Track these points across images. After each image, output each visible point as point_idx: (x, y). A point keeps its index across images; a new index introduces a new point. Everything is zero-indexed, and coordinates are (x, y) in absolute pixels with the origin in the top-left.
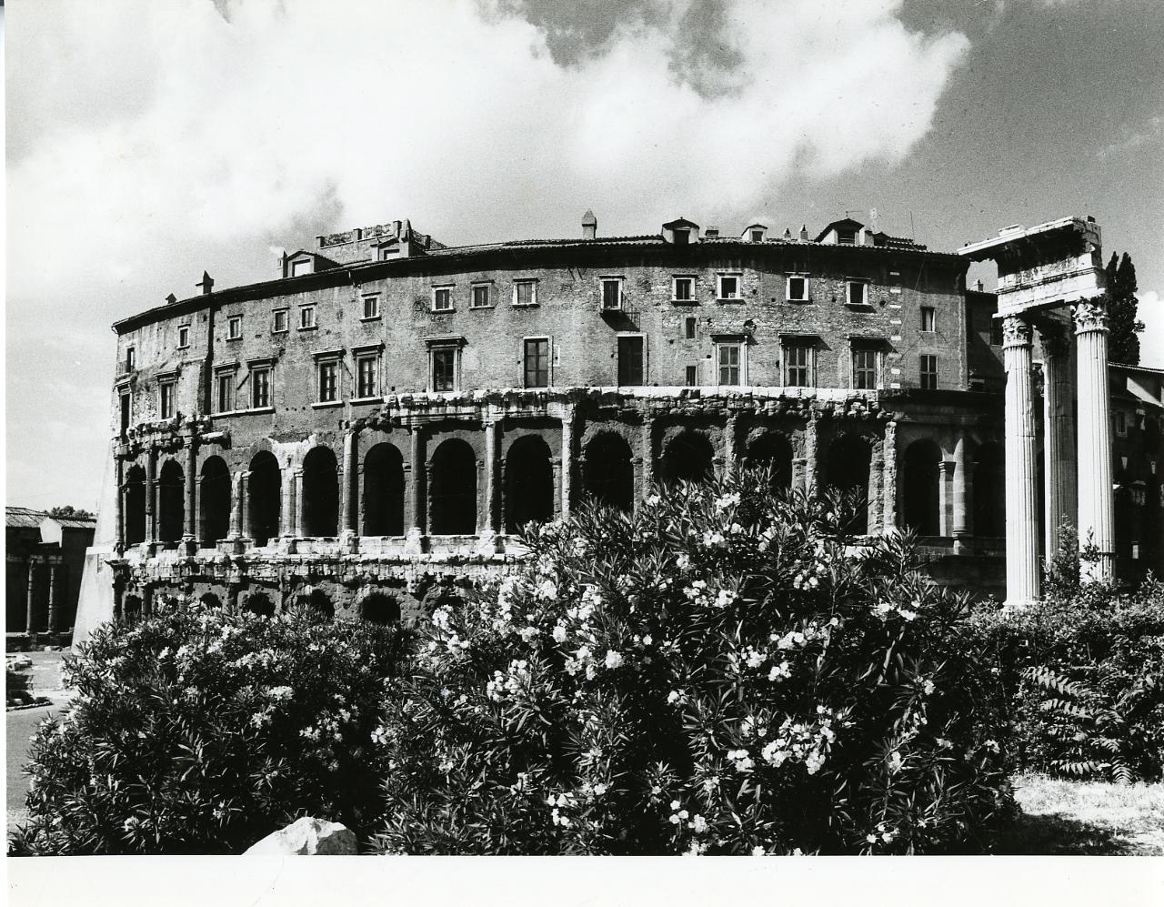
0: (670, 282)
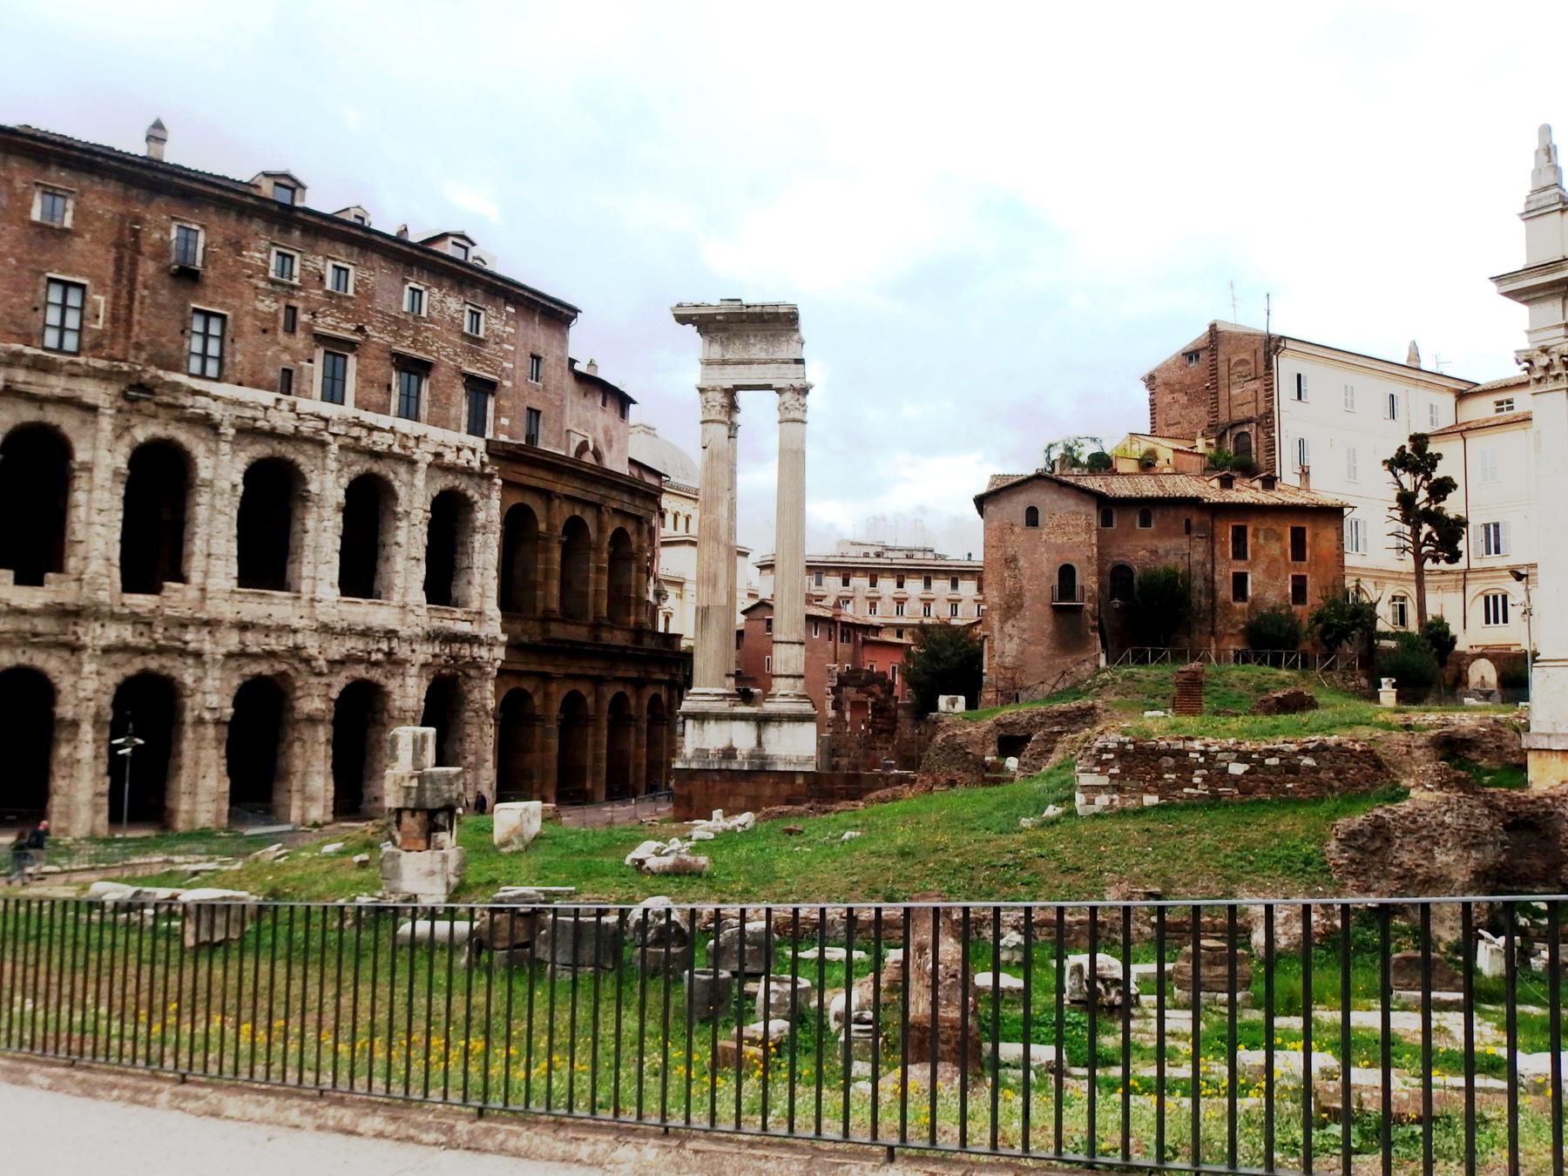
0: (268, 251)
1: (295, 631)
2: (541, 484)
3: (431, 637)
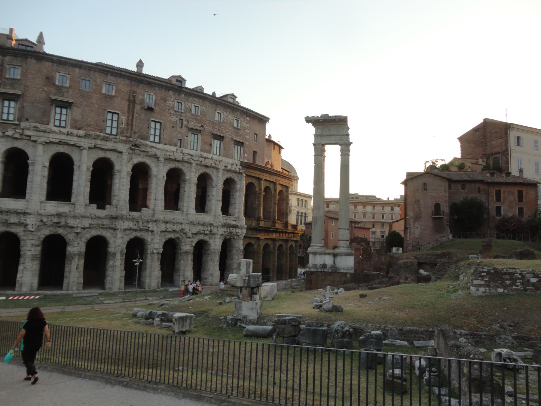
0: (174, 101)
1: (182, 224)
2: (257, 176)
3: (224, 226)
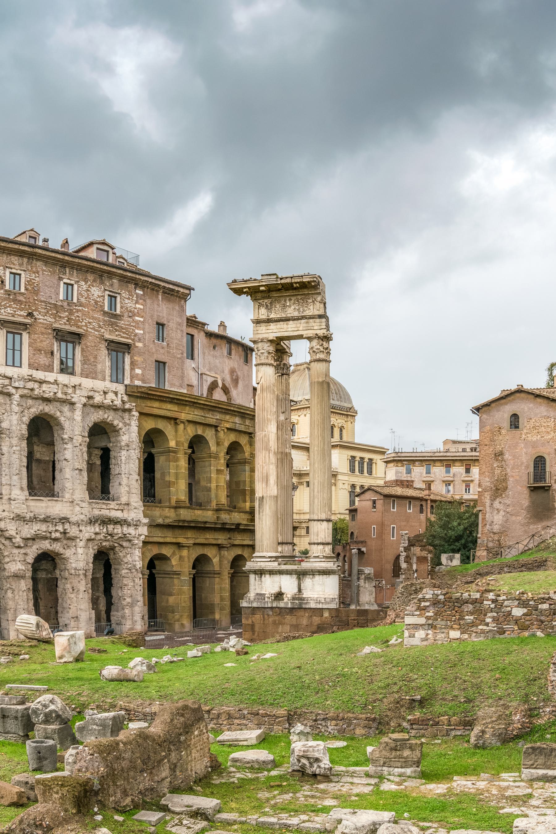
3: (92, 521)
